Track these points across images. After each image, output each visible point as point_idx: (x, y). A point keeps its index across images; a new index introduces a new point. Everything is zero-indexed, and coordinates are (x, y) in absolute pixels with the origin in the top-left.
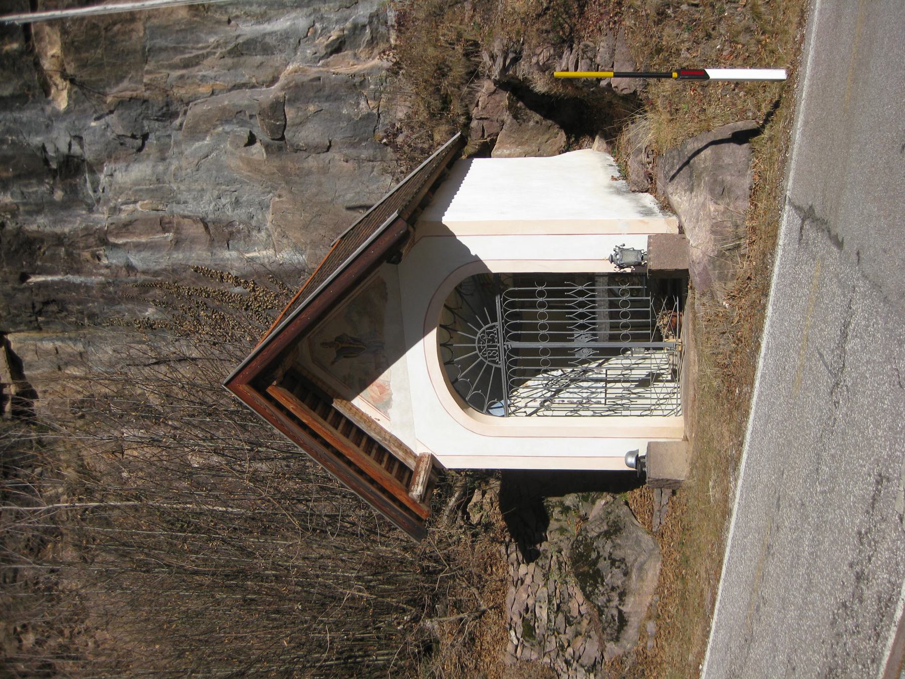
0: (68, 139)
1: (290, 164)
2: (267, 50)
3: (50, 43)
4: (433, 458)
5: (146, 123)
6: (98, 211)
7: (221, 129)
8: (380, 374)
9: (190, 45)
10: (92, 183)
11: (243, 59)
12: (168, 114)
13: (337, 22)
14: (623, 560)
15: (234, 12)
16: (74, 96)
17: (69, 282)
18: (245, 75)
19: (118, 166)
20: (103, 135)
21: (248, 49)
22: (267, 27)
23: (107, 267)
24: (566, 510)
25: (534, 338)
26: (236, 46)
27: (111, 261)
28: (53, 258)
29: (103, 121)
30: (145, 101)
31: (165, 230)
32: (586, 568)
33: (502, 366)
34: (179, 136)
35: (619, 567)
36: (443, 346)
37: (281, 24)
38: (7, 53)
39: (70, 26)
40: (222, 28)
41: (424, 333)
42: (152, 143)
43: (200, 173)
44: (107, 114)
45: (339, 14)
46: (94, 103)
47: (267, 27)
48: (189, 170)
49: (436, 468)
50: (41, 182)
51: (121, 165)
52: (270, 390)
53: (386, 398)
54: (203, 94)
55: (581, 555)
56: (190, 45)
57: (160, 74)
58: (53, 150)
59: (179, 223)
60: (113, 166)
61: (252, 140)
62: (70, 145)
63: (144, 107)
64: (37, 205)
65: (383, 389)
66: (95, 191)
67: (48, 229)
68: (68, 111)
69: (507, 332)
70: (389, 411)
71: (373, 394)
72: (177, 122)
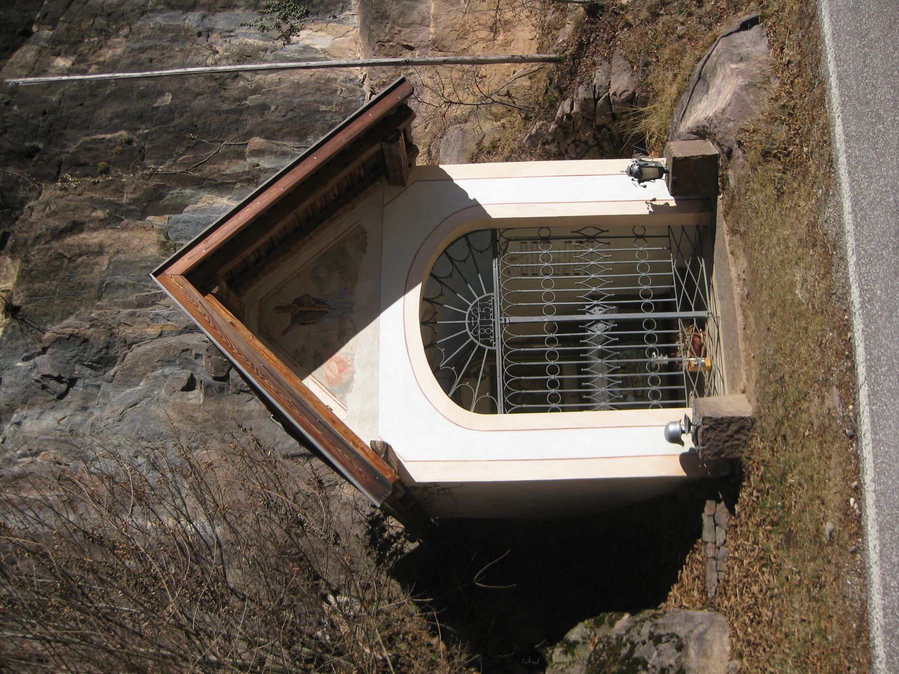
1: (228, 406)
5: (78, 367)
7: (160, 371)
8: (343, 344)
12: (103, 362)
16: (10, 331)
19: (30, 412)
20: (26, 376)
29: (31, 362)
30: (86, 341)
33: (498, 348)
35: (668, 641)
36: (427, 321)
39: (34, 256)
41: (406, 291)
42: (78, 391)
43: (122, 424)
44: (39, 354)
46: (29, 341)
48: (110, 420)
51: (36, 410)
54: (150, 335)
60: (24, 413)
61: (190, 386)
63: (81, 348)
65: (343, 366)
70: (348, 397)
71: (329, 373)
72: (112, 372)
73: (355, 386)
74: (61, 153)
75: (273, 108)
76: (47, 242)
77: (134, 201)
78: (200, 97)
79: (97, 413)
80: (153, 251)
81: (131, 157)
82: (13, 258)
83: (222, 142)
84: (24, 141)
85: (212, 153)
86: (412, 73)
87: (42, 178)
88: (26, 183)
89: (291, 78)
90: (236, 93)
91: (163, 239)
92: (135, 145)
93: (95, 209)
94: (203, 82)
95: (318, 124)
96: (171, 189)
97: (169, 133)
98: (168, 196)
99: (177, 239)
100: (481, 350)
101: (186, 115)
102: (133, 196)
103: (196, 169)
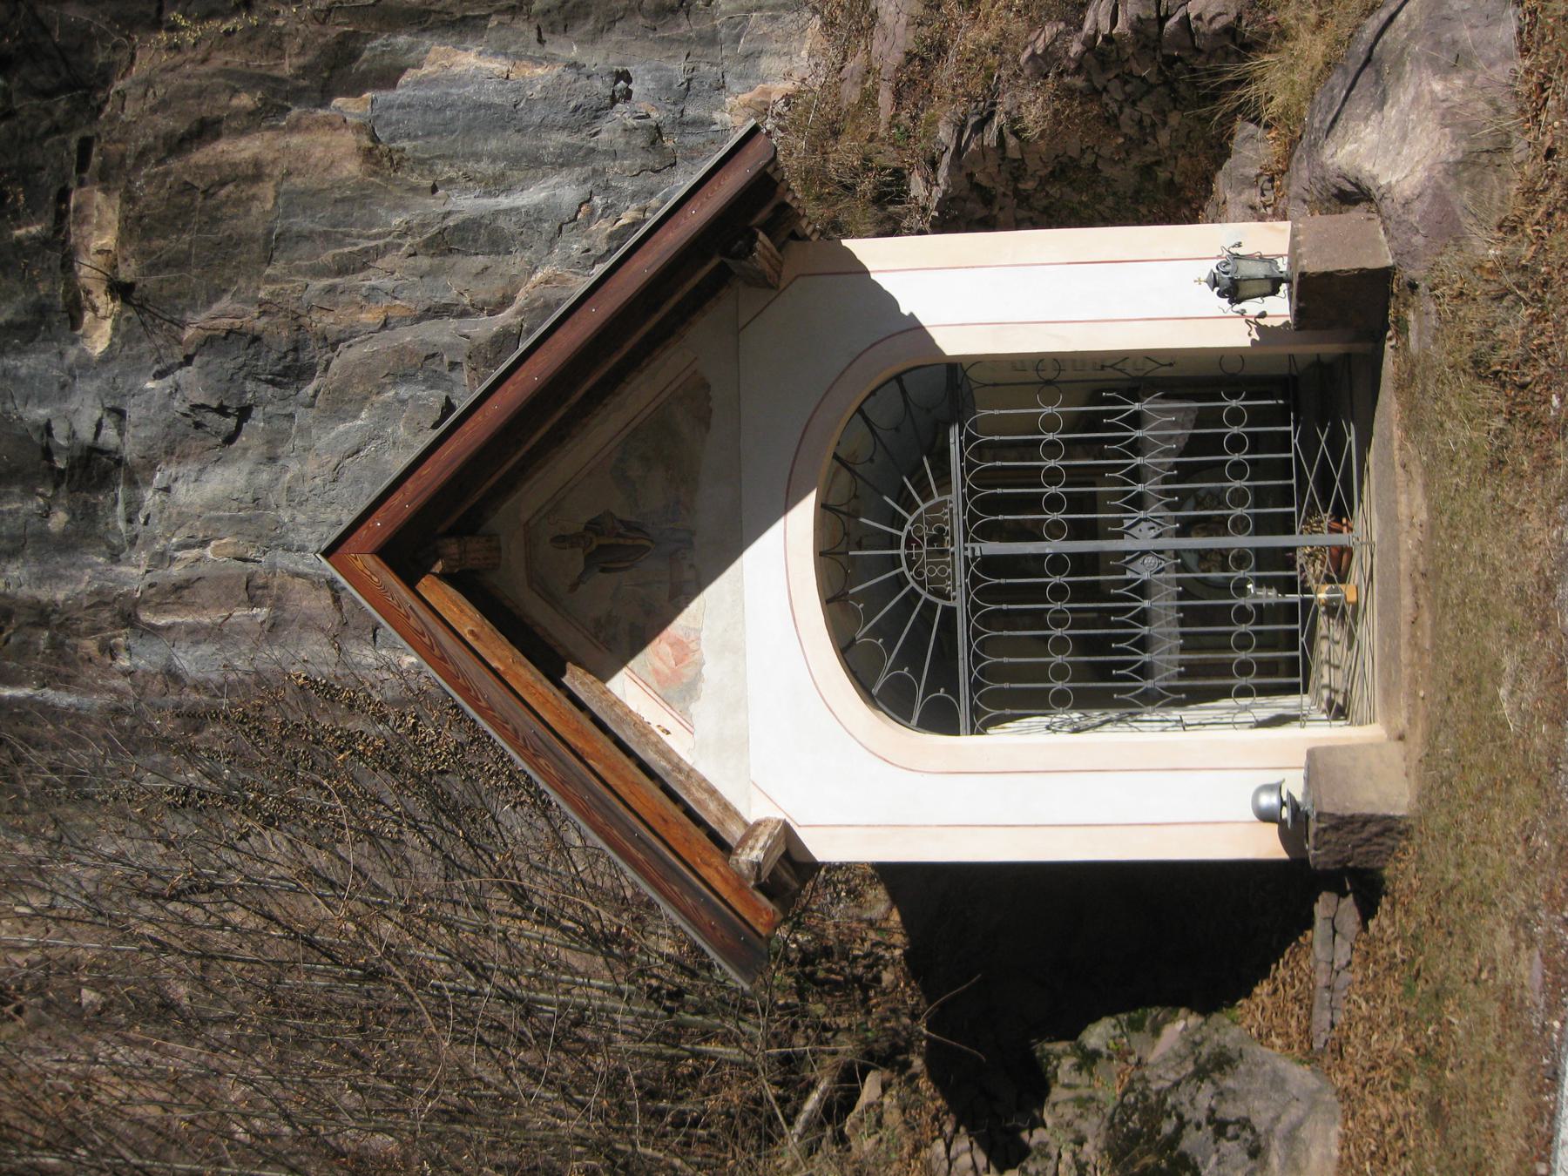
0: (98, 413)
2: (498, 243)
3: (100, 227)
4: (787, 834)
5: (250, 386)
6: (128, 562)
7: (392, 393)
8: (679, 610)
9: (354, 231)
10: (128, 504)
11: (450, 260)
12: (293, 373)
13: (634, 196)
14: (1244, 1123)
15: (446, 171)
17: (44, 704)
18: (451, 289)
19: (182, 470)
20: (165, 407)
21: (462, 240)
22: (504, 202)
23: (127, 673)
24: (1089, 1059)
25: (1036, 537)
26: (441, 232)
27: (136, 660)
28: (24, 650)
29: (169, 380)
30: (256, 339)
31: (253, 602)
32: (1150, 1160)
33: (960, 603)
35: (1236, 1137)
37: (531, 196)
38: (19, 241)
39: (141, 188)
40: (419, 199)
41: (786, 509)
42: (255, 427)
44: (181, 365)
45: (639, 182)
46: (160, 342)
47: (504, 202)
48: (317, 481)
50: (30, 493)
51: (191, 467)
52: (427, 585)
53: (689, 672)
54: (366, 325)
55: (1134, 1137)
56: (354, 231)
57: (294, 282)
58: (65, 433)
59: (282, 587)
60: (173, 470)
62: (99, 426)
63: (251, 351)
64: (12, 538)
65: (683, 651)
66: (130, 521)
67: (25, 592)
68: (107, 358)
69: (973, 518)
70: (694, 708)
71: (658, 664)
72: (310, 389)
73: (706, 689)
76: (160, 162)
77: (305, 71)
79: (294, 467)
80: (352, 168)
82: (106, 191)
88: (103, 36)
91: (367, 143)
96: (369, 38)
98: (366, 54)
99: (393, 139)
102: (302, 61)
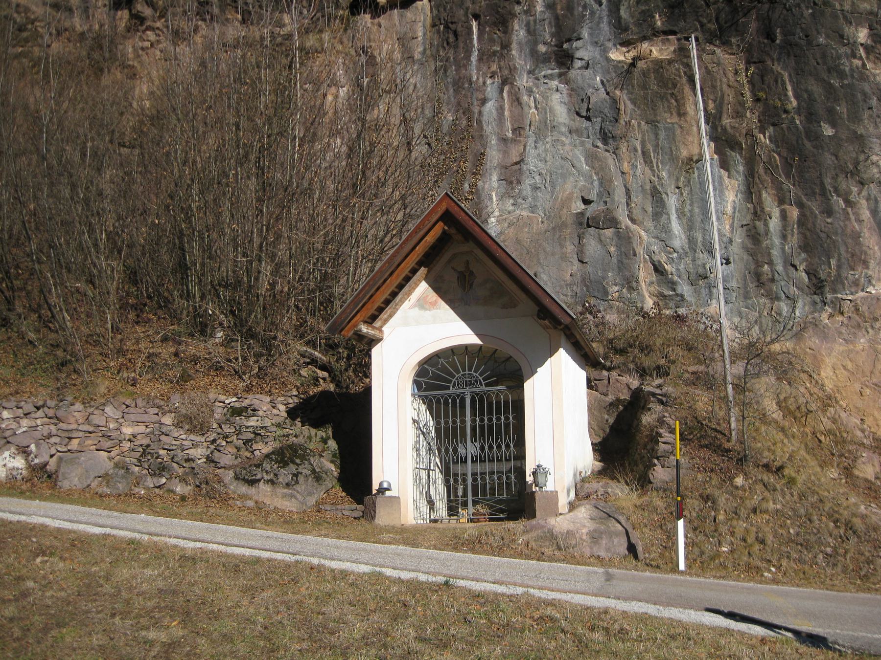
0: (586, 58)
1: (568, 231)
2: (656, 216)
3: (661, 50)
4: (380, 340)
5: (599, 119)
6: (528, 78)
8: (446, 302)
9: (660, 157)
10: (551, 75)
11: (650, 197)
12: (605, 137)
13: (678, 270)
14: (297, 482)
15: (685, 193)
16: (620, 65)
17: (472, 51)
18: (637, 199)
19: (565, 95)
20: (589, 86)
21: (657, 201)
22: (674, 217)
23: (484, 83)
24: (324, 441)
25: (473, 414)
26: (659, 192)
27: (490, 86)
28: (492, 41)
29: (601, 86)
30: (617, 121)
31: (514, 130)
32: (288, 455)
33: (452, 391)
34: (589, 146)
36: (466, 349)
37: (676, 227)
38: (654, 17)
40: (673, 182)
41: (478, 335)
43: (560, 160)
44: (606, 90)
45: (684, 271)
47: (674, 217)
49: (373, 342)
50: (553, 35)
51: (566, 99)
52: (441, 224)
53: (427, 306)
55: (296, 451)
56: (660, 157)
57: (638, 133)
58: (578, 46)
59: (520, 141)
60: (565, 92)
61: (586, 202)
62: (581, 59)
64: (535, 30)
65: (434, 304)
66: (544, 77)
67: (514, 38)
68: (608, 60)
69: (477, 394)
70: (417, 309)
72: (599, 144)
73: (422, 312)
74: (773, 60)
75: (829, 220)
76: (685, 73)
77: (724, 130)
78: (833, 158)
79: (567, 141)
80: (684, 153)
81: (771, 116)
82: (675, 51)
83: (794, 185)
84: (781, 27)
85: (783, 179)
86: (868, 332)
87: (748, 51)
88: (743, 40)
89: (865, 230)
90: (843, 186)
91: (695, 159)
92: (784, 116)
93: (715, 101)
94: (851, 157)
95: (817, 260)
96: (740, 154)
97: (797, 141)
98: (733, 154)
99: (698, 169)
100: (450, 382)
101: (815, 150)
102: (728, 127)
103: (766, 170)
